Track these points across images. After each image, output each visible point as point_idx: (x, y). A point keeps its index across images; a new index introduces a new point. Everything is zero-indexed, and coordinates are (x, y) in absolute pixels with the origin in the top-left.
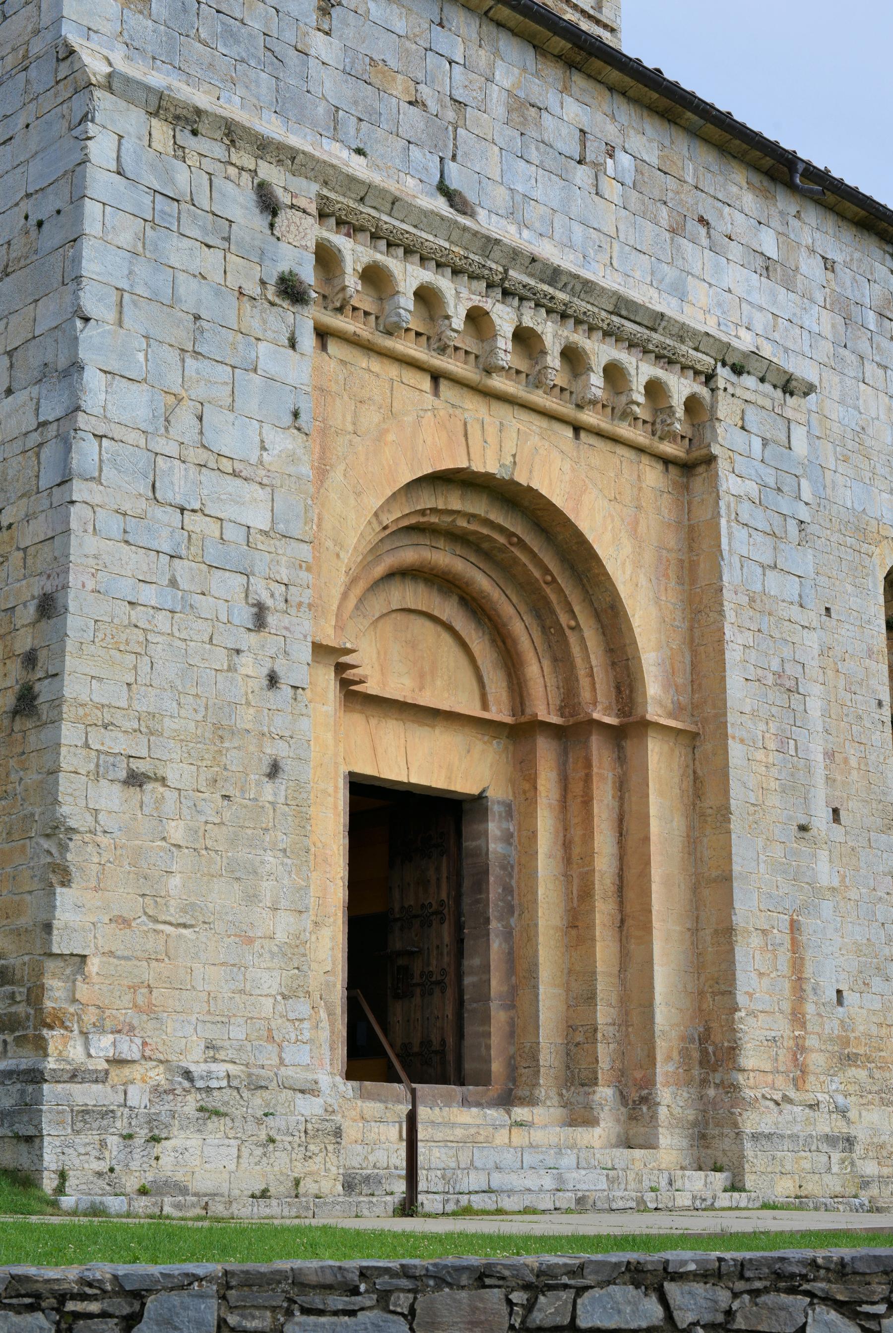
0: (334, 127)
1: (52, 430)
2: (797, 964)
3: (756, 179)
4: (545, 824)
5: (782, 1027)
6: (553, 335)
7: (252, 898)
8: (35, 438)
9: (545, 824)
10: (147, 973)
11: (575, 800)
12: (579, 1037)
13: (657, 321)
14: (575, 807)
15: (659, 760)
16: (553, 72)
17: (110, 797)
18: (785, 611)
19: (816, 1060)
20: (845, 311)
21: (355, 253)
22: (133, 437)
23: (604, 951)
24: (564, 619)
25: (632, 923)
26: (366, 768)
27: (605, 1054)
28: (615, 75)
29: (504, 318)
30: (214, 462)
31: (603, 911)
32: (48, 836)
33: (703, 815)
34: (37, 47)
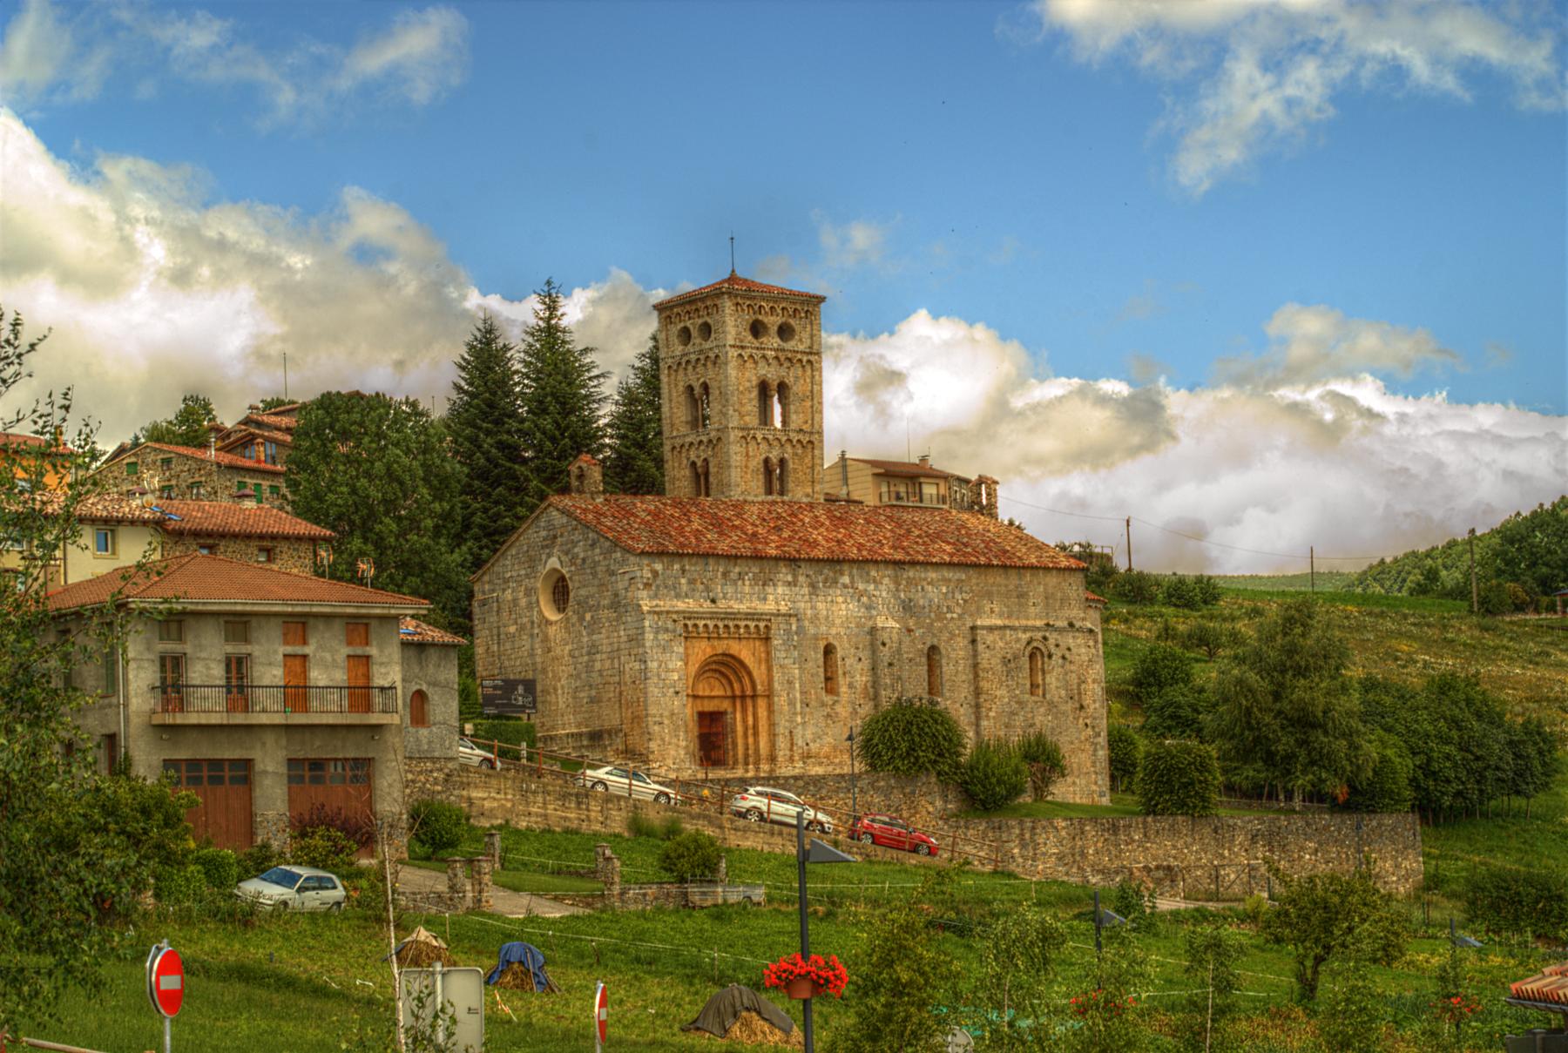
4: (738, 716)
6: (731, 624)
9: (738, 716)
11: (744, 711)
12: (746, 756)
15: (762, 703)
17: (656, 728)
20: (813, 586)
23: (751, 740)
25: (756, 734)
27: (751, 760)
29: (721, 624)
31: (750, 732)
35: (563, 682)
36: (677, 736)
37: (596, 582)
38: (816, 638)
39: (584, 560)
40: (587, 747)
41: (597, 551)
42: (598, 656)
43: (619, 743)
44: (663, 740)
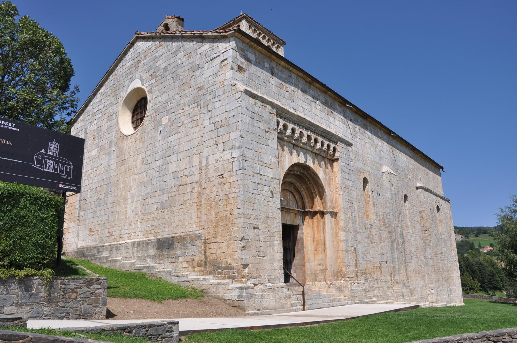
0: (274, 97)
1: (236, 159)
2: (356, 256)
3: (339, 104)
5: (353, 268)
6: (313, 136)
7: (274, 251)
8: (231, 160)
10: (258, 266)
13: (329, 133)
14: (315, 227)
16: (308, 85)
18: (352, 188)
19: (359, 274)
21: (282, 122)
22: (251, 160)
24: (313, 190)
26: (284, 222)
28: (318, 85)
30: (263, 164)
32: (240, 241)
33: (339, 228)
34: (226, 83)
35: (134, 191)
36: (272, 246)
37: (177, 84)
38: (360, 171)
39: (165, 69)
40: (153, 257)
41: (182, 54)
42: (174, 158)
43: (195, 252)
44: (258, 248)
